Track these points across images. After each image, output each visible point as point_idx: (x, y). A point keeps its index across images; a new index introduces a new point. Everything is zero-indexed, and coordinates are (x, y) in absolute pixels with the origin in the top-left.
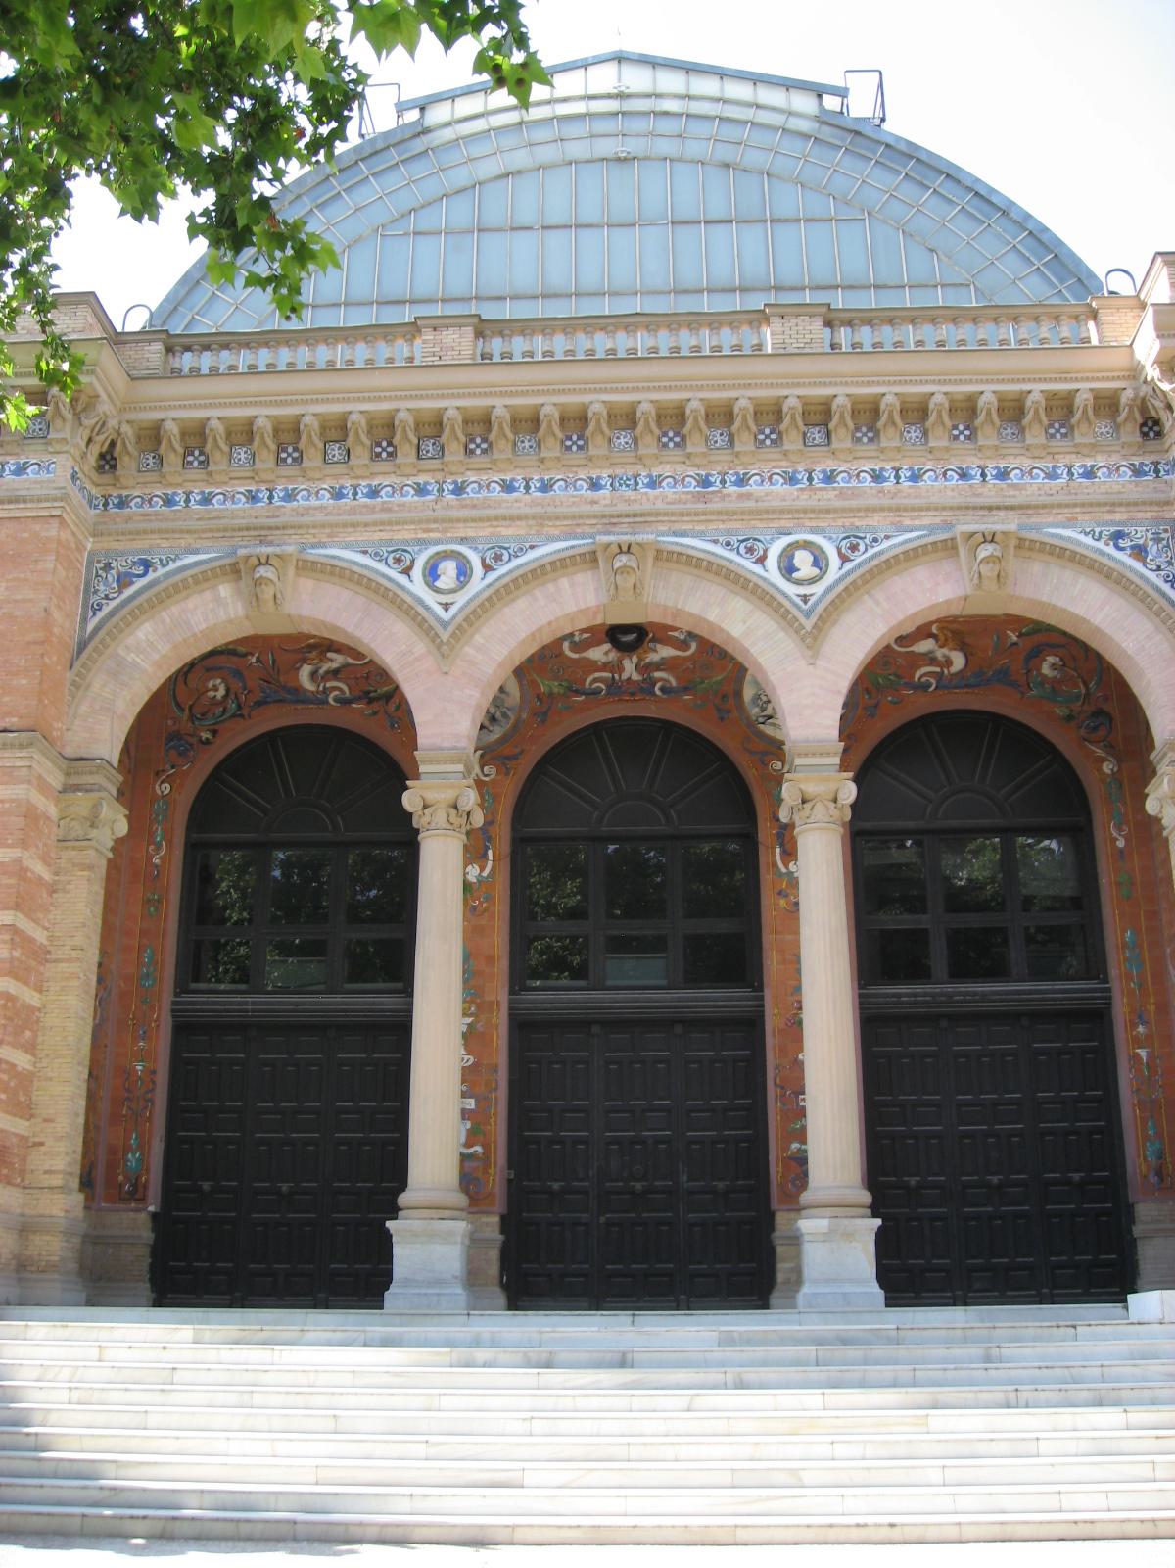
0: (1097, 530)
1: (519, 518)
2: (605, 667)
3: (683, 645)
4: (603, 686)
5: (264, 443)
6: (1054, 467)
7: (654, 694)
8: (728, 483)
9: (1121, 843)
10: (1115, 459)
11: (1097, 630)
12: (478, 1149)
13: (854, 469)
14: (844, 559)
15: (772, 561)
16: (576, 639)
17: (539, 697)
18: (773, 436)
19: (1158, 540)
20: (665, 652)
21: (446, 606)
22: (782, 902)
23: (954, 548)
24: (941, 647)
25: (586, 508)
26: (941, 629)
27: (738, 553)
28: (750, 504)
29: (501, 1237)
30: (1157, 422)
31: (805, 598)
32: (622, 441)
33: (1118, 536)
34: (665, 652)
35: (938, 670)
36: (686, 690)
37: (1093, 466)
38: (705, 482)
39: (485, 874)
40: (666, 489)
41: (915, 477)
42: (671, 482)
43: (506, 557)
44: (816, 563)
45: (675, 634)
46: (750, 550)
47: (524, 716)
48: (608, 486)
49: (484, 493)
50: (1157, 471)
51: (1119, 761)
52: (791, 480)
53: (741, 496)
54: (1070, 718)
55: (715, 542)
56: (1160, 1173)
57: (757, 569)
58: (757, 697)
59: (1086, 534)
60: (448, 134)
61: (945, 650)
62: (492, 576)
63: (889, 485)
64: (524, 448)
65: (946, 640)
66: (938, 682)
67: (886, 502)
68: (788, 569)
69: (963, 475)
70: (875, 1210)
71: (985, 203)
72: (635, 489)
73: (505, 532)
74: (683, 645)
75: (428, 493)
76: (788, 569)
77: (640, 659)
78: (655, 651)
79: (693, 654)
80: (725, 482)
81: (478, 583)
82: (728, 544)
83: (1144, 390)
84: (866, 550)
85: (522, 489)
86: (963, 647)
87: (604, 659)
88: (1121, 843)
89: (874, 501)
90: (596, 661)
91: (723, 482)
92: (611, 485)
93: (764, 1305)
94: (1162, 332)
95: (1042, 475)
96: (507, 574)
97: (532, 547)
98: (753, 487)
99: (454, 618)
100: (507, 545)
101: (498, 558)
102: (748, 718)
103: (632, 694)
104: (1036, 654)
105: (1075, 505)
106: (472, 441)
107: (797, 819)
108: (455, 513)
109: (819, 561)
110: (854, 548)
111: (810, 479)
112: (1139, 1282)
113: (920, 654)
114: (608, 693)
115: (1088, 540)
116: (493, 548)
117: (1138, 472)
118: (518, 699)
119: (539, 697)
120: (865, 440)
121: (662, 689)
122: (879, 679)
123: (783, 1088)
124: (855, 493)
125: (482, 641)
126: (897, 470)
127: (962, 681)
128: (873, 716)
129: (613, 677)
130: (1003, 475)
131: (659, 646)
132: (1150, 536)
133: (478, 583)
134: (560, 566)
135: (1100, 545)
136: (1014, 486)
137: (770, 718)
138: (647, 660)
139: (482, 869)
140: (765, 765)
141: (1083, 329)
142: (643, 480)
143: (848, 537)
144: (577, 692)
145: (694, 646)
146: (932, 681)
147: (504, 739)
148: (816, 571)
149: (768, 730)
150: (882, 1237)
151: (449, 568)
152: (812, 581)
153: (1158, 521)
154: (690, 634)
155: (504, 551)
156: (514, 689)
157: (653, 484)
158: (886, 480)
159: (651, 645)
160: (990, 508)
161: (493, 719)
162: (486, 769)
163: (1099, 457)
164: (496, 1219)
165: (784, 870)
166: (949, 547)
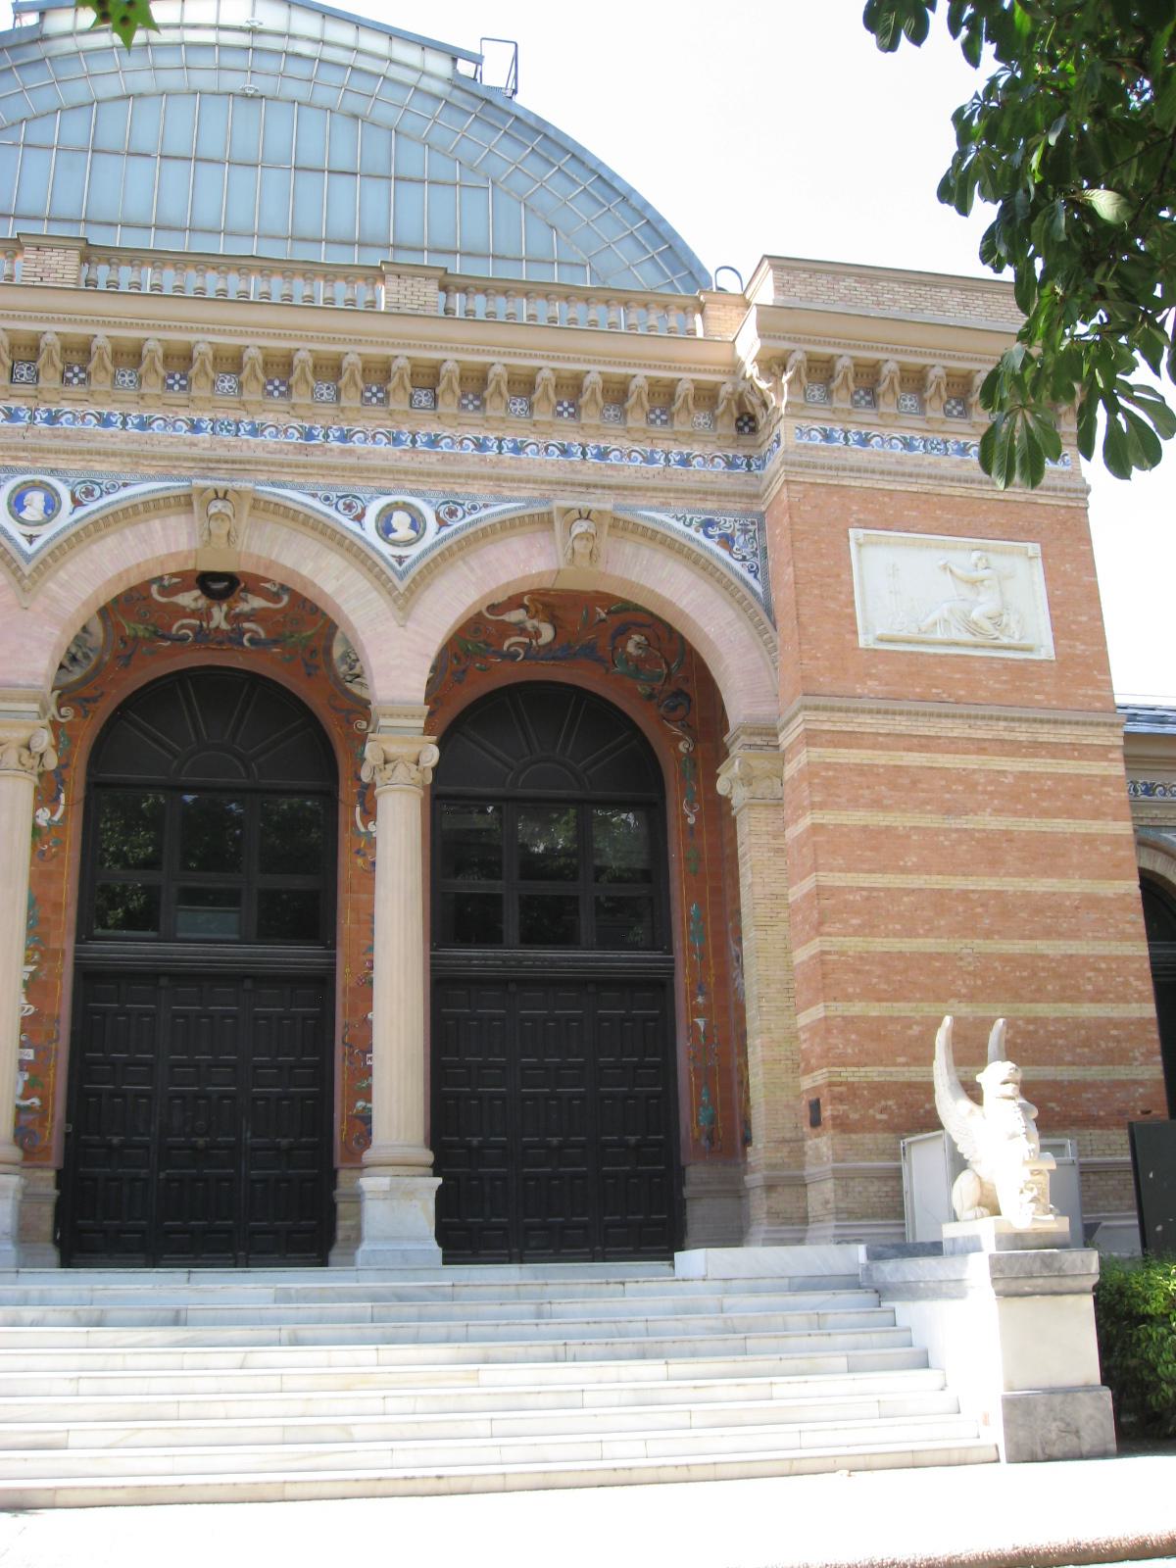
0: (689, 517)
1: (114, 454)
2: (194, 613)
3: (274, 597)
4: (191, 634)
5: (50, 361)
6: (652, 452)
7: (242, 644)
8: (331, 438)
9: (691, 820)
10: (709, 450)
11: (682, 614)
12: (36, 1101)
13: (458, 436)
14: (442, 524)
15: (370, 520)
16: (166, 583)
17: (124, 640)
18: (380, 395)
19: (745, 532)
20: (257, 603)
21: (31, 539)
22: (360, 861)
23: (551, 522)
24: (532, 618)
25: (186, 450)
26: (530, 600)
27: (337, 508)
28: (351, 461)
29: (56, 1192)
30: (752, 418)
31: (400, 560)
32: (226, 384)
33: (707, 524)
34: (257, 603)
35: (527, 640)
36: (275, 642)
37: (689, 454)
38: (309, 435)
39: (56, 818)
40: (268, 438)
41: (518, 449)
42: (272, 432)
43: (97, 493)
44: (413, 526)
45: (267, 585)
46: (349, 507)
47: (107, 658)
48: (209, 430)
49: (79, 425)
50: (749, 465)
51: (695, 740)
52: (395, 440)
53: (343, 452)
54: (651, 697)
55: (314, 496)
56: (711, 1138)
57: (354, 526)
58: (345, 656)
59: (678, 519)
60: (68, 45)
61: (535, 622)
62: (81, 512)
63: (491, 454)
64: (124, 382)
65: (537, 612)
66: (526, 654)
67: (486, 470)
68: (386, 529)
69: (565, 452)
70: (437, 1169)
71: (607, 188)
72: (237, 435)
73: (98, 467)
74: (274, 597)
75: (20, 419)
76: (386, 529)
77: (231, 608)
78: (246, 601)
79: (285, 607)
80: (328, 437)
81: (66, 517)
82: (327, 499)
83: (743, 386)
84: (464, 516)
85: (118, 424)
86: (553, 620)
87: (193, 605)
88: (691, 820)
89: (475, 469)
90: (184, 608)
91: (326, 436)
92: (212, 429)
93: (324, 1262)
94: (763, 332)
95: (640, 459)
96: (98, 510)
97: (125, 485)
98: (356, 444)
99: (38, 551)
100: (99, 481)
101: (89, 493)
102: (336, 676)
103: (220, 643)
104: (623, 632)
105: (669, 490)
106: (70, 369)
107: (377, 778)
108: (46, 443)
109: (417, 524)
110: (452, 513)
111: (414, 441)
112: (688, 1241)
113: (510, 623)
114: (195, 641)
115: (679, 526)
116: (84, 482)
117: (731, 464)
118: (101, 641)
119: (124, 640)
120: (471, 407)
121: (251, 640)
122: (470, 644)
123: (351, 1046)
124: (457, 459)
125: (66, 578)
126: (500, 440)
127: (549, 653)
128: (460, 682)
129: (201, 626)
130: (603, 455)
131: (250, 596)
132: (737, 526)
133: (66, 517)
134: (153, 506)
135: (691, 531)
136: (612, 467)
137: (358, 676)
138: (237, 610)
139: (53, 813)
140: (350, 723)
141: (690, 321)
142: (245, 427)
143: (447, 502)
144: (164, 638)
145: (286, 599)
146: (521, 651)
147: (85, 681)
148: (413, 534)
149: (355, 689)
150: (441, 1195)
151: (36, 500)
152: (409, 543)
153: (746, 513)
154: (282, 587)
155: (96, 487)
156: (97, 628)
157: (256, 431)
158: (489, 449)
159: (242, 595)
160: (588, 486)
161: (74, 659)
162: (63, 710)
163: (695, 446)
164: (51, 1174)
165: (363, 830)
166: (545, 521)
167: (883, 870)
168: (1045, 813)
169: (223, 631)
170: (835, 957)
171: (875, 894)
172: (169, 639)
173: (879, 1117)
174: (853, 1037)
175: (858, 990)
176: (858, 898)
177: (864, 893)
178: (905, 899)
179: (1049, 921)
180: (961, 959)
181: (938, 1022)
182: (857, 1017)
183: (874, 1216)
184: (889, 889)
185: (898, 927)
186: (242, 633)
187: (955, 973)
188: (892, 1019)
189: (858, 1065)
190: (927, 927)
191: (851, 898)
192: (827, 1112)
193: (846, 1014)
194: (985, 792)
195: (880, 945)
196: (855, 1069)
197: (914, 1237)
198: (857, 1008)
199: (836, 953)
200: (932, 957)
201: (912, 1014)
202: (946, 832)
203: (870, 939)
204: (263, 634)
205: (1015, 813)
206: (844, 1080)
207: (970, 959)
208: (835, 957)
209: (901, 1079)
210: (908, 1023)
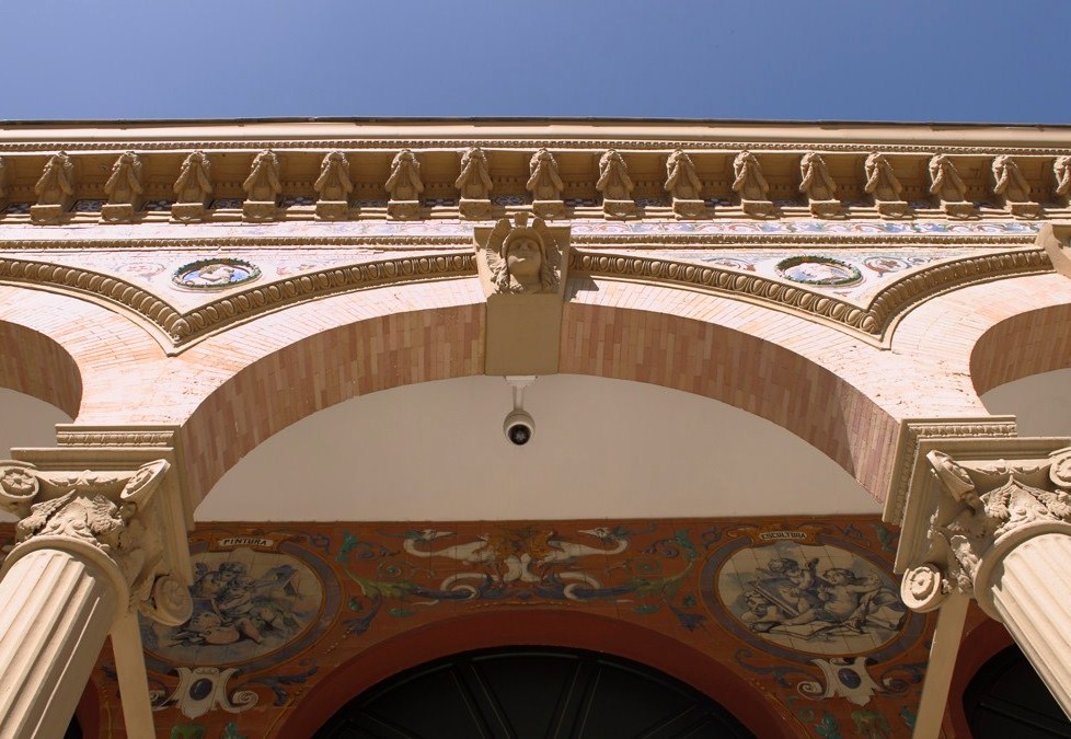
2: (474, 567)
4: (472, 589)
20: (578, 550)
34: (578, 550)
74: (607, 543)
77: (535, 558)
87: (474, 558)
118: (318, 604)
129: (490, 579)
131: (564, 545)
138: (547, 559)
141: (1000, 192)
145: (623, 545)
159: (553, 543)
169: (527, 584)
172: (436, 597)
186: (564, 584)
204: (596, 585)
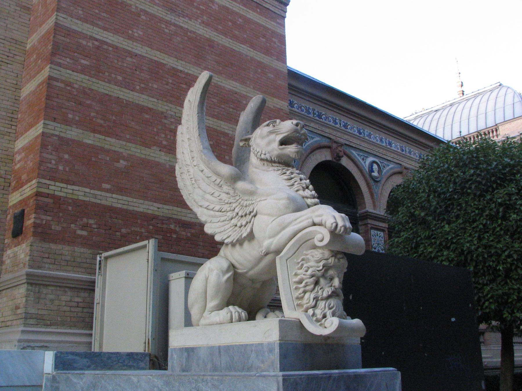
167: (116, 32)
168: (235, 38)
170: (62, 85)
171: (105, 47)
173: (79, 232)
174: (66, 156)
175: (77, 118)
176: (90, 44)
177: (96, 43)
178: (129, 59)
179: (231, 110)
180: (166, 118)
181: (191, 81)
182: (73, 141)
183: (63, 324)
184: (117, 48)
185: (120, 78)
187: (160, 127)
188: (102, 149)
189: (67, 182)
190: (143, 85)
191: (84, 43)
192: (29, 221)
193: (62, 135)
194: (198, 8)
195: (102, 87)
196: (64, 185)
197: (101, 347)
198: (73, 133)
199: (63, 82)
200: (143, 109)
201: (121, 150)
202: (168, 23)
203: (94, 80)
205: (217, 30)
206: (51, 192)
207: (173, 120)
208: (62, 85)
209: (104, 202)
210: (117, 156)
